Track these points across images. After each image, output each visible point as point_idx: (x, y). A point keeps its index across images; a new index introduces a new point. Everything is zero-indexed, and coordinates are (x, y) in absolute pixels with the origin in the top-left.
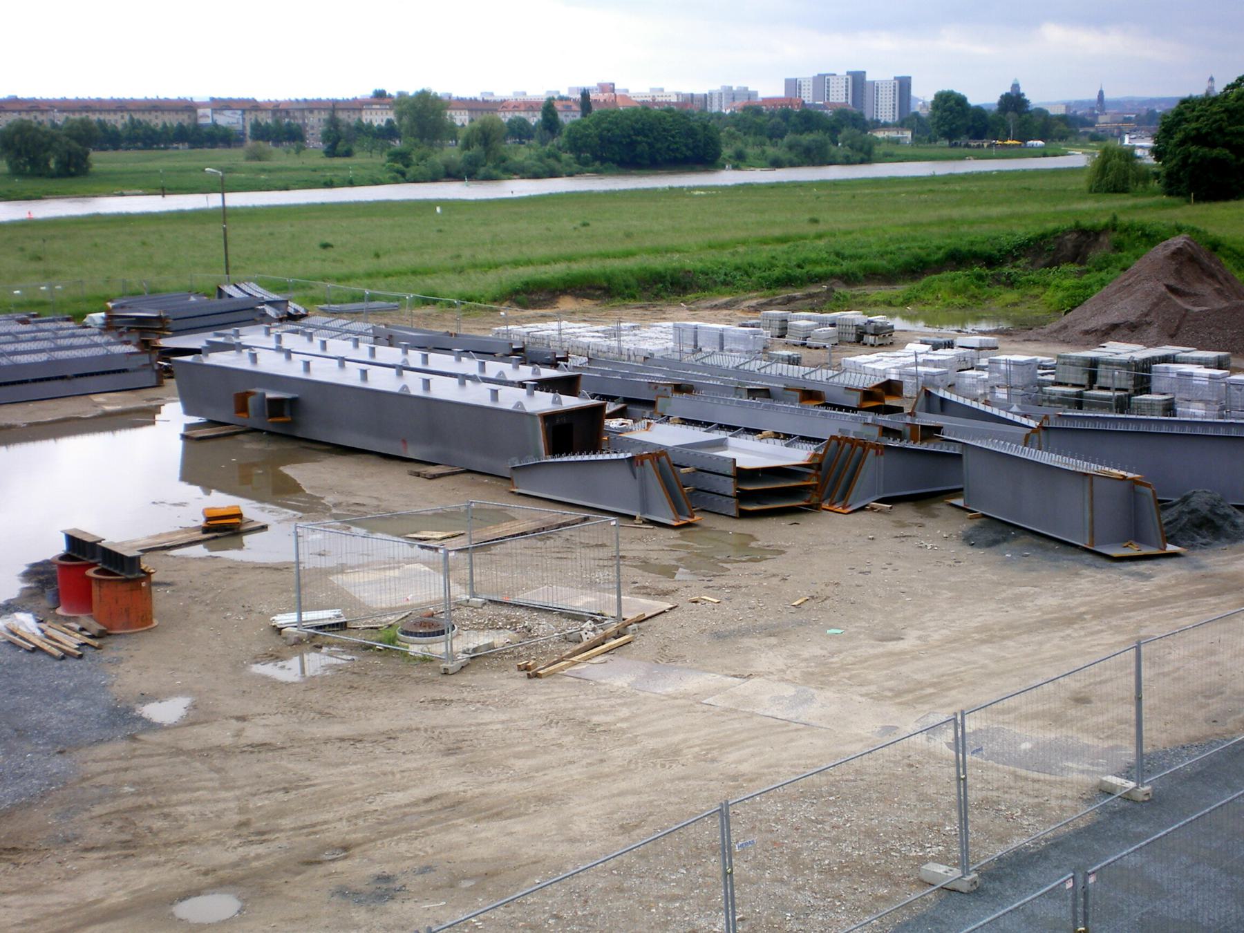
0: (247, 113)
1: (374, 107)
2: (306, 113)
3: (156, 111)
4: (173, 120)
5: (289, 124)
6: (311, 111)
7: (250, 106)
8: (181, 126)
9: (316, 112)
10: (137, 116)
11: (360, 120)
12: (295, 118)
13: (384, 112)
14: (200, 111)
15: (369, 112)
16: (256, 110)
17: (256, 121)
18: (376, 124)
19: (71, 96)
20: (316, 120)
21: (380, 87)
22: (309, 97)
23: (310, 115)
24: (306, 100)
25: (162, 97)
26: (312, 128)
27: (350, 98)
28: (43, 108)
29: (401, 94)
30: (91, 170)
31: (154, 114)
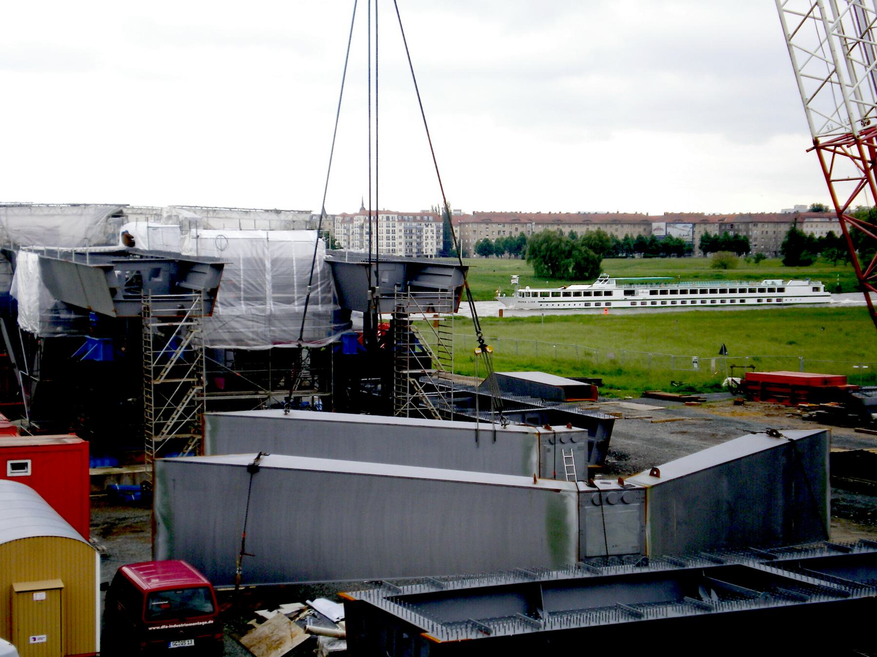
2: (751, 226)
3: (617, 224)
4: (635, 232)
5: (736, 236)
6: (755, 224)
8: (640, 238)
10: (603, 229)
11: (802, 230)
12: (738, 230)
13: (824, 225)
14: (655, 225)
15: (809, 225)
16: (705, 224)
17: (707, 233)
19: (545, 211)
20: (759, 233)
22: (753, 212)
23: (754, 228)
24: (750, 215)
25: (621, 212)
26: (756, 239)
27: (779, 211)
28: (523, 221)
31: (614, 227)
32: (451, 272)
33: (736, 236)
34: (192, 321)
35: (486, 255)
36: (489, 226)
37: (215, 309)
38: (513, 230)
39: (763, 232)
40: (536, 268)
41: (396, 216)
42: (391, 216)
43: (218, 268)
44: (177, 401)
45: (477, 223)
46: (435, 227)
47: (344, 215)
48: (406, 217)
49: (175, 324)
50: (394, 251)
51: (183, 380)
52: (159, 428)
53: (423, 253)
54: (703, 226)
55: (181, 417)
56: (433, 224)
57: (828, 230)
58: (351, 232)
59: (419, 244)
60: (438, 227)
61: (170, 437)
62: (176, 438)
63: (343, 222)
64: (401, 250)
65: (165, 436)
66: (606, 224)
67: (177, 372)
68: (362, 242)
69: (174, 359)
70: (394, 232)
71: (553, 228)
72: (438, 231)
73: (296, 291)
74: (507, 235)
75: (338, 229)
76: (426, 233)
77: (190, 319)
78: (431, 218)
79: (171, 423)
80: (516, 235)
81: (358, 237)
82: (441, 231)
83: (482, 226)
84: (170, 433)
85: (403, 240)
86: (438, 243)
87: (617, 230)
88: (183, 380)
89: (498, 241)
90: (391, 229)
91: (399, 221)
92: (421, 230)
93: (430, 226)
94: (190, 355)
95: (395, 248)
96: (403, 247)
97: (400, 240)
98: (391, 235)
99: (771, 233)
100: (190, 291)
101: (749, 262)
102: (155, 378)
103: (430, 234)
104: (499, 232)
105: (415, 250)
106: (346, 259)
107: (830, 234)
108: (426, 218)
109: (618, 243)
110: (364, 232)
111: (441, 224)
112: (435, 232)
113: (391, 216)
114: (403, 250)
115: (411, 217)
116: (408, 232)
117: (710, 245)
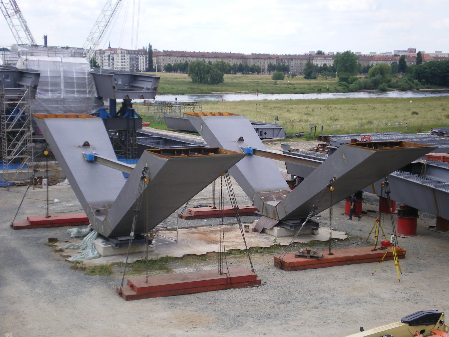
0: (266, 60)
1: (318, 58)
2: (290, 61)
3: (230, 58)
4: (238, 62)
5: (284, 65)
6: (292, 60)
7: (268, 57)
8: (241, 65)
9: (294, 60)
11: (312, 63)
12: (285, 62)
13: (322, 60)
15: (316, 60)
16: (270, 59)
17: (271, 63)
18: (319, 66)
19: (197, 51)
20: (294, 64)
21: (320, 49)
22: (291, 54)
23: (291, 62)
24: (290, 55)
25: (232, 52)
26: (292, 67)
27: (302, 54)
28: (187, 55)
29: (338, 53)
30: (223, 82)
31: (229, 59)
32: (152, 80)
33: (284, 65)
34: (24, 101)
35: (169, 72)
36: (171, 57)
37: (36, 95)
38: (182, 59)
39: (295, 63)
40: (192, 78)
41: (126, 51)
42: (123, 51)
43: (38, 75)
44: (18, 140)
45: (165, 56)
46: (144, 57)
47: (100, 50)
48: (130, 52)
49: (16, 102)
50: (125, 68)
51: (21, 130)
52: (10, 152)
53: (139, 69)
54: (269, 60)
55: (21, 147)
56: (144, 56)
57: (324, 63)
58: (104, 58)
59: (137, 65)
60: (146, 57)
61: (15, 157)
62: (19, 158)
63: (100, 54)
64: (128, 68)
65: (13, 156)
66: (225, 58)
67: (19, 125)
68: (109, 64)
69: (16, 119)
70: (125, 59)
71: (201, 60)
72: (146, 59)
73: (75, 87)
74: (179, 62)
75: (97, 57)
76: (140, 60)
77: (24, 100)
78: (143, 53)
79: (15, 150)
80: (183, 62)
81: (107, 61)
82: (148, 59)
83: (167, 57)
84: (15, 155)
85: (129, 63)
86: (146, 65)
87: (230, 61)
88: (21, 130)
89: (175, 65)
90: (123, 57)
91: (127, 54)
92: (137, 59)
93: (142, 57)
94: (23, 118)
95: (126, 67)
96: (129, 66)
99: (299, 64)
100: (23, 86)
101: (289, 77)
102: (7, 128)
103: (142, 61)
104: (175, 60)
105: (135, 68)
106: (101, 72)
107: (325, 65)
108: (140, 53)
109: (230, 67)
110: (110, 59)
111: (148, 56)
112: (145, 59)
113: (123, 51)
114: (129, 68)
115: (133, 52)
116: (132, 59)
117: (271, 68)
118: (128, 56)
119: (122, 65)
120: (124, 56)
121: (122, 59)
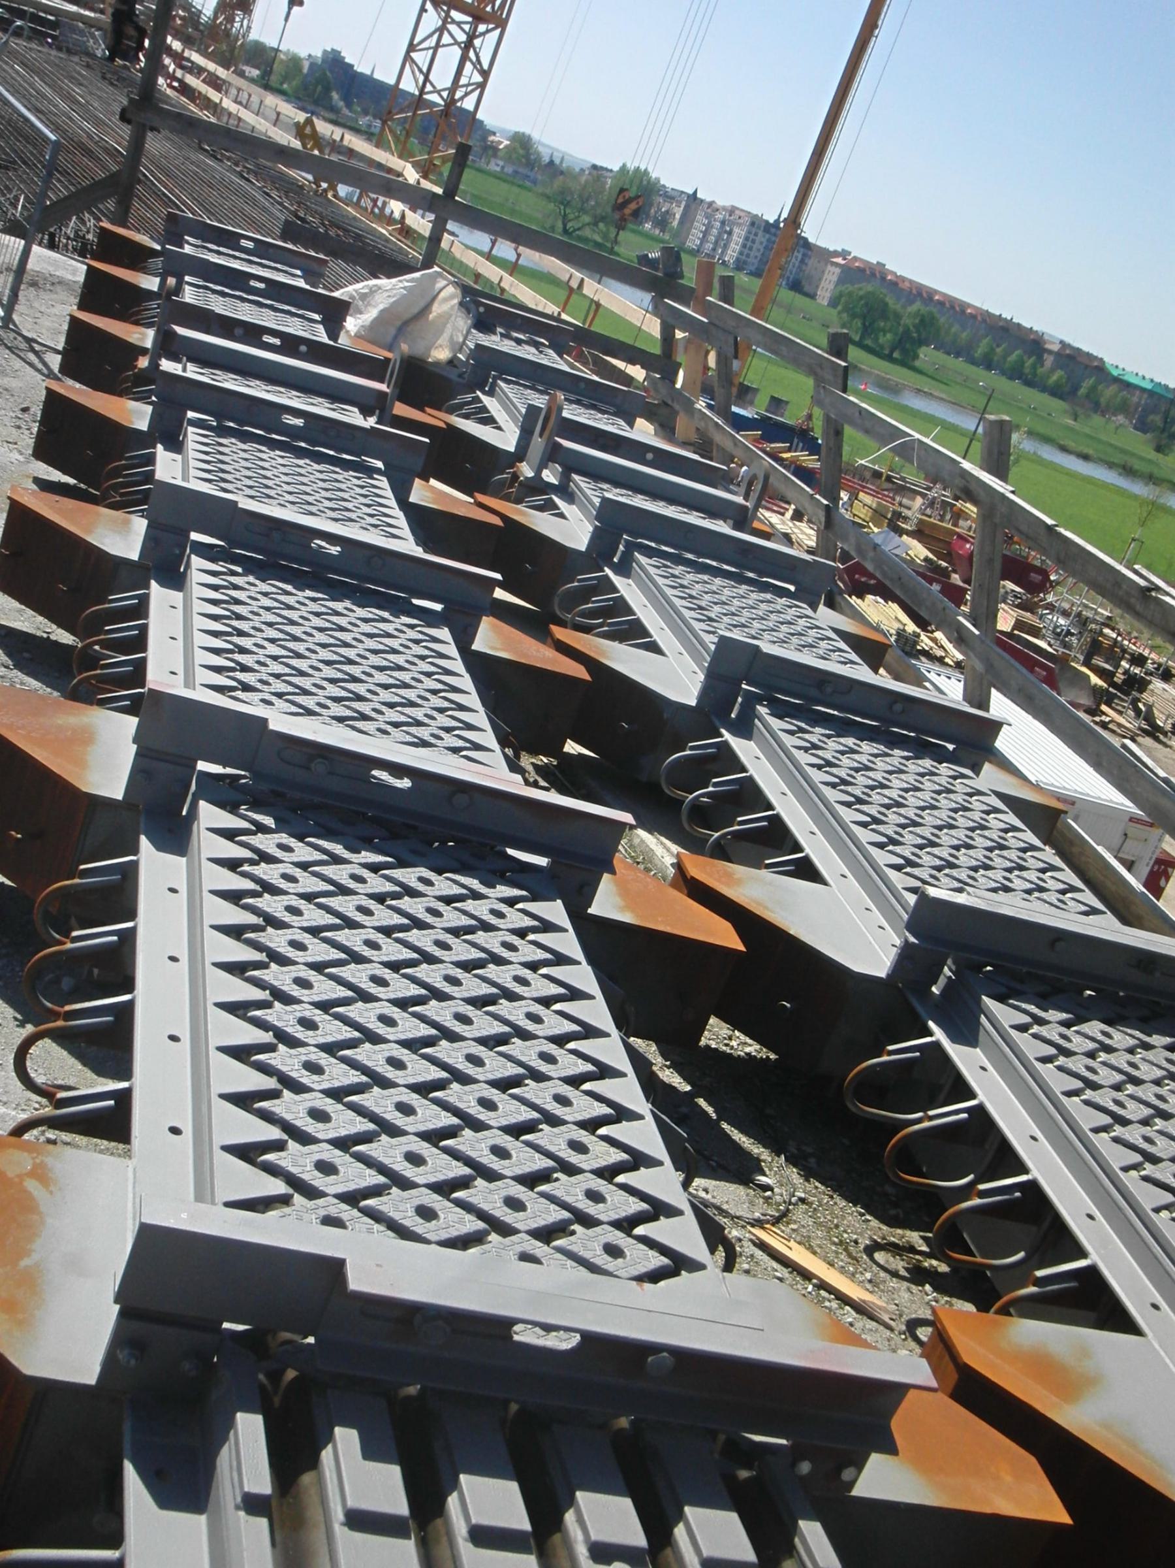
70: (753, 241)
85: (759, 255)
90: (752, 237)
95: (749, 260)
96: (756, 262)
97: (757, 254)
98: (749, 244)
112: (799, 260)
118: (764, 236)
119: (741, 253)
120: (756, 235)
121: (747, 239)
